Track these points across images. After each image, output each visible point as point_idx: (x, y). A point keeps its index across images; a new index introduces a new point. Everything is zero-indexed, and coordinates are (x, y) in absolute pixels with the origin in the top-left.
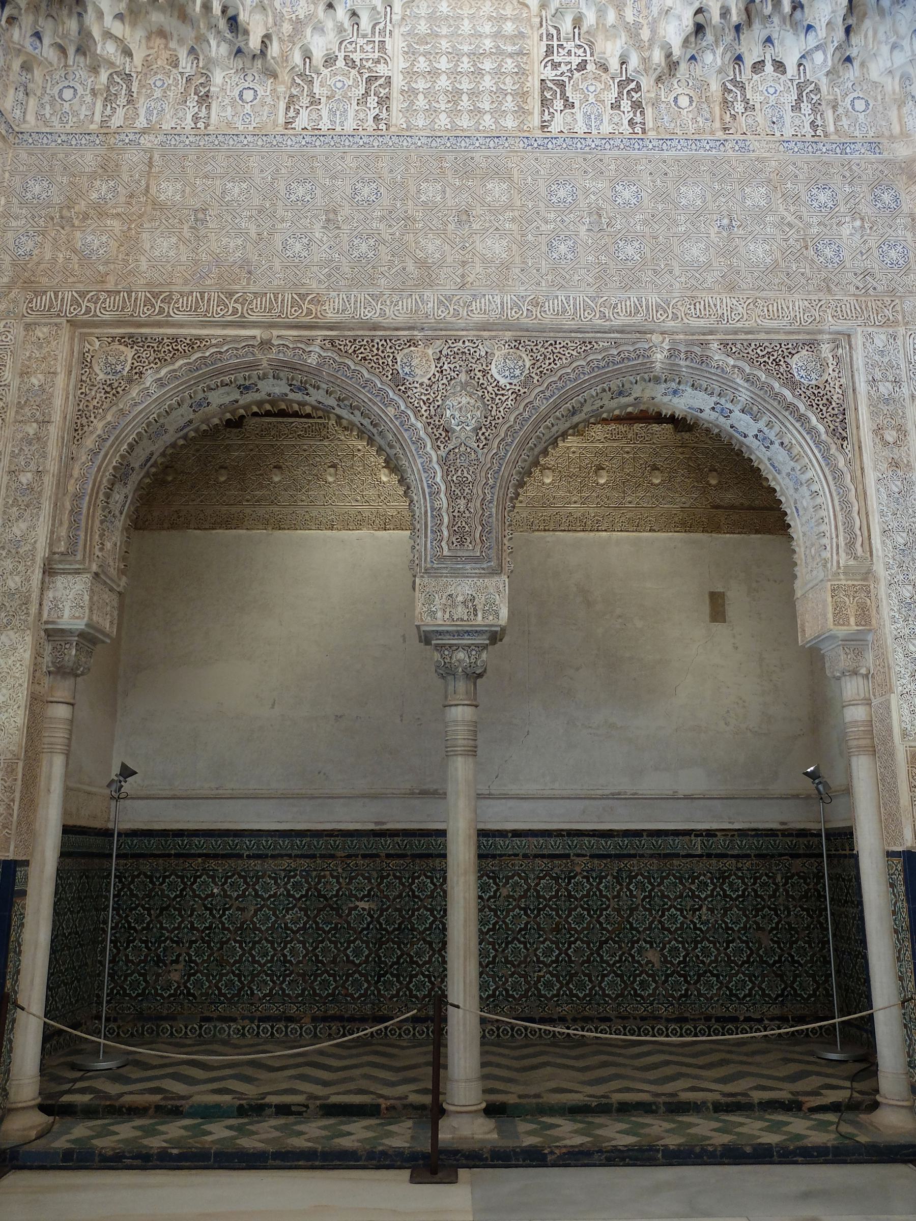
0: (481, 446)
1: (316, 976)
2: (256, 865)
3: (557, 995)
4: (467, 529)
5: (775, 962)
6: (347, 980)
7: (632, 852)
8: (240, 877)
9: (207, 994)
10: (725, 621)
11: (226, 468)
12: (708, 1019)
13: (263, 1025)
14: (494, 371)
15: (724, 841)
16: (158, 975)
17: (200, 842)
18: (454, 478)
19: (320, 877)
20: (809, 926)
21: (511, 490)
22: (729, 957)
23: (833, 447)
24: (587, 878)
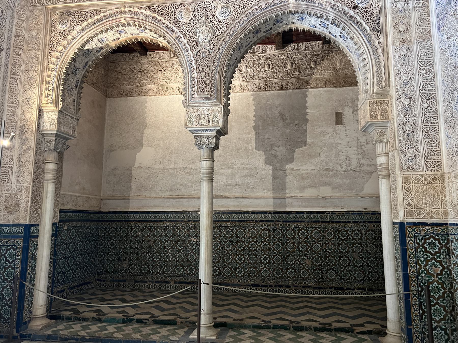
0: (211, 49)
1: (176, 266)
2: (154, 224)
3: (269, 276)
4: (205, 85)
5: (360, 266)
6: (188, 268)
7: (300, 220)
8: (149, 229)
9: (136, 272)
10: (342, 125)
11: (141, 72)
12: (331, 288)
13: (156, 284)
14: (217, 15)
15: (339, 216)
16: (119, 265)
17: (133, 216)
18: (200, 63)
19: (178, 229)
20: (376, 252)
21: (225, 67)
22: (340, 263)
23: (373, 36)
24: (281, 230)
